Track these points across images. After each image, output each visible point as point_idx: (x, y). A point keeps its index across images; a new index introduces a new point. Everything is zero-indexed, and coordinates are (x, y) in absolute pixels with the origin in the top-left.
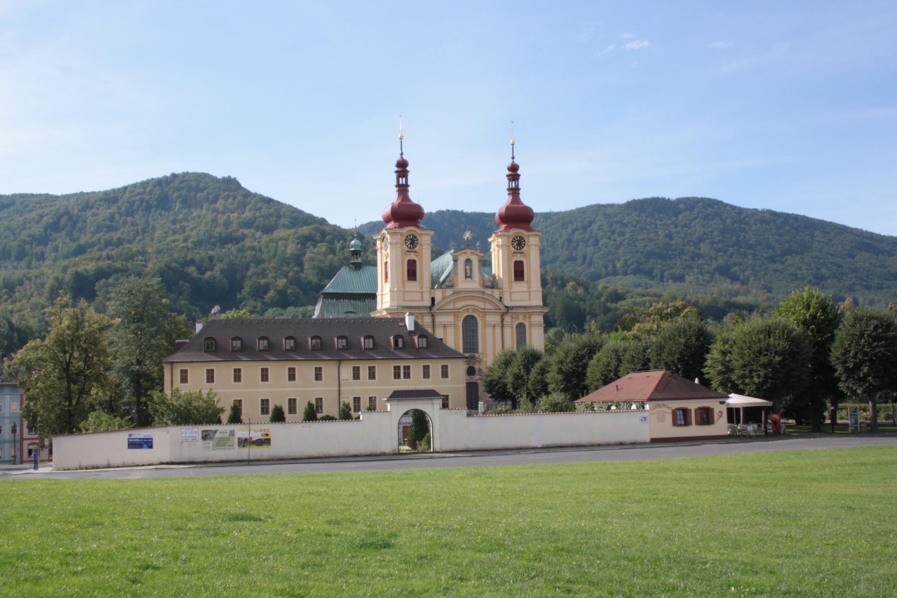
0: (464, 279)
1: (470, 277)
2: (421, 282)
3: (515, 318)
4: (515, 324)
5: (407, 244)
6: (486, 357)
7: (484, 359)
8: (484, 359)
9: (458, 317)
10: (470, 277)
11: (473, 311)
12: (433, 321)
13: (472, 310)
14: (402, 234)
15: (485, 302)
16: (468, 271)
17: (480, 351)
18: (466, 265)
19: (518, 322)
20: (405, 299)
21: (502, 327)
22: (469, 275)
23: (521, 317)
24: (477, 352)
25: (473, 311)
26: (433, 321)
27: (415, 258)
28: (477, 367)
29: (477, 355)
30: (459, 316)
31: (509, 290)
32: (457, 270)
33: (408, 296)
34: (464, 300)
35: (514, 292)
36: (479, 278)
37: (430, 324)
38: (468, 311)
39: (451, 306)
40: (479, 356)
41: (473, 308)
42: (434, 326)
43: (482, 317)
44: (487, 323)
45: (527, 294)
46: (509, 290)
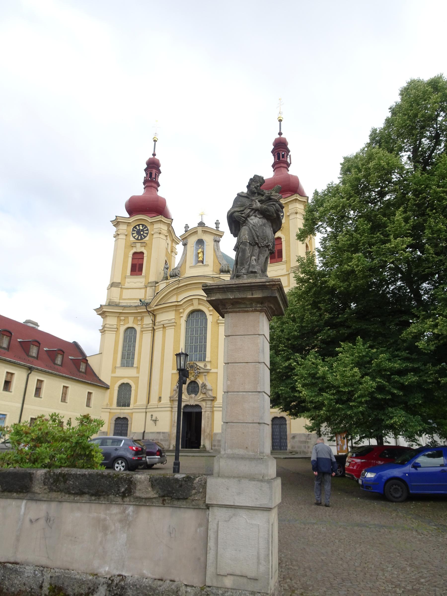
0: (193, 264)
1: (202, 262)
5: (134, 235)
6: (217, 368)
7: (213, 370)
8: (213, 370)
11: (199, 304)
13: (197, 300)
18: (197, 249)
22: (201, 259)
25: (199, 304)
28: (200, 381)
29: (201, 365)
30: (181, 311)
32: (186, 255)
33: (127, 294)
34: (190, 289)
37: (151, 325)
38: (192, 304)
39: (174, 299)
40: (205, 366)
41: (199, 299)
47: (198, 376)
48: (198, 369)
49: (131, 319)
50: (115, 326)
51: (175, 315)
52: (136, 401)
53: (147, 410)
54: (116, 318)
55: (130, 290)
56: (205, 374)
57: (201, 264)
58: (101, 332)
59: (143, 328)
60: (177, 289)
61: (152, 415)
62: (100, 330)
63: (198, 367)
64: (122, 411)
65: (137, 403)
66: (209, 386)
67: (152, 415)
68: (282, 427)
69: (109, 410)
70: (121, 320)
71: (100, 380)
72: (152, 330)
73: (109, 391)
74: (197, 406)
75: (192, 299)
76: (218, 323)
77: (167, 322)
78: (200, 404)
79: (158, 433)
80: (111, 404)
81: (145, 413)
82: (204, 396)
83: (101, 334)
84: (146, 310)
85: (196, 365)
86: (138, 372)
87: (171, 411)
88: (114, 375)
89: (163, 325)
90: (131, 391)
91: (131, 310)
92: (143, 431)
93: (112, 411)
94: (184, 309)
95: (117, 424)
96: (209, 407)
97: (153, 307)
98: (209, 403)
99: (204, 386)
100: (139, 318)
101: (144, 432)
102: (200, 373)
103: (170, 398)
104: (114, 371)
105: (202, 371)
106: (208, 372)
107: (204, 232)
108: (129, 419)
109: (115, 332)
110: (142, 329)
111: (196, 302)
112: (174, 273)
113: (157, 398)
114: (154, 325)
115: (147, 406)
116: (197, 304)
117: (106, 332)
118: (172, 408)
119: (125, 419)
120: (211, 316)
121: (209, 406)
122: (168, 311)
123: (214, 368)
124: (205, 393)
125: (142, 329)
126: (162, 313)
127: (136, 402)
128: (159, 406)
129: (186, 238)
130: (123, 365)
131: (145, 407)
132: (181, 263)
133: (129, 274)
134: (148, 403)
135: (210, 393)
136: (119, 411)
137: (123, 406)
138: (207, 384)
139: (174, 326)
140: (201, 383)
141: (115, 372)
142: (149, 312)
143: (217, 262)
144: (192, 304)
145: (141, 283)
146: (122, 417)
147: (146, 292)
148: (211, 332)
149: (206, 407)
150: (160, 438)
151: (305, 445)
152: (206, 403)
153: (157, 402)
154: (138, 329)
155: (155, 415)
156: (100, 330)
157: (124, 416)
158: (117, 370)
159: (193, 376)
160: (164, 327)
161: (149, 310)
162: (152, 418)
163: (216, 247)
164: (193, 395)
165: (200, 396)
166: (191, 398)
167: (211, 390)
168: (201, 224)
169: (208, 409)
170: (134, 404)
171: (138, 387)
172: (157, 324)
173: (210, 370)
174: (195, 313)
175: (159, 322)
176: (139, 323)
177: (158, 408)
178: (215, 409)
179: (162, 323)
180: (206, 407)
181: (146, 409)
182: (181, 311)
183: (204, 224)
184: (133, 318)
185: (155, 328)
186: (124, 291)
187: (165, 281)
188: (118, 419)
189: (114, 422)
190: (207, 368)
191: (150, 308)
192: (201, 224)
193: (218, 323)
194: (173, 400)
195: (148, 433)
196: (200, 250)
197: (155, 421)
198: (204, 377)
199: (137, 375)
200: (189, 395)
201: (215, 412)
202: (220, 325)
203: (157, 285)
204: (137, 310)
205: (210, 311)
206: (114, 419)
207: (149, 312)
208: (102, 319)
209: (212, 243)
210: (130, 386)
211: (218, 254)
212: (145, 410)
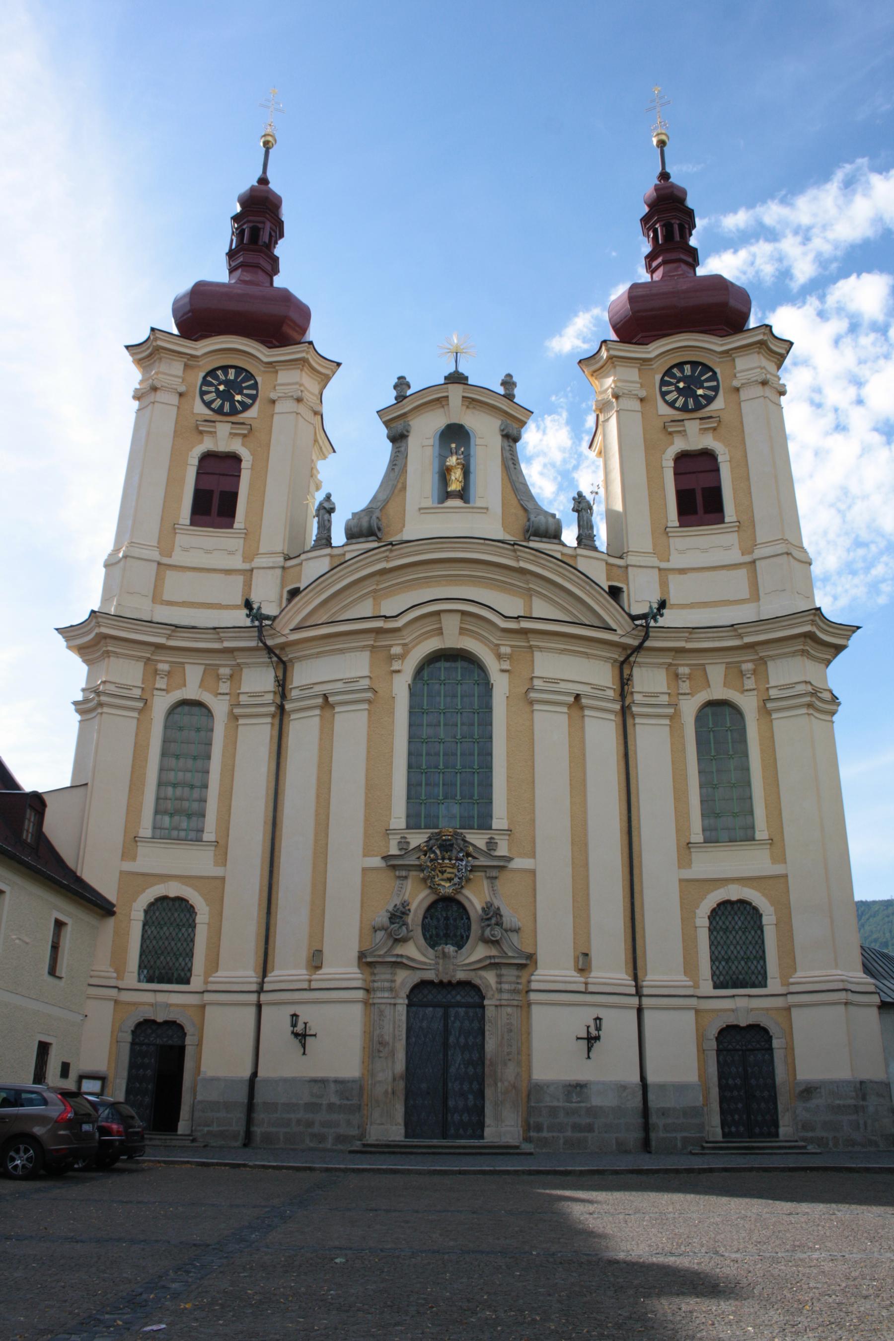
2: (251, 536)
3: (690, 677)
4: (689, 708)
6: (533, 856)
8: (519, 863)
9: (392, 658)
10: (463, 495)
11: (463, 631)
12: (282, 685)
14: (190, 361)
15: (529, 594)
16: (457, 475)
17: (500, 820)
19: (703, 697)
20: (166, 597)
21: (625, 713)
23: (716, 672)
24: (485, 823)
25: (463, 631)
26: (282, 685)
27: (236, 446)
29: (478, 839)
30: (396, 650)
31: (655, 561)
32: (404, 470)
34: (427, 581)
35: (682, 571)
36: (504, 504)
37: (269, 698)
38: (440, 632)
40: (492, 844)
41: (463, 613)
42: (281, 708)
43: (510, 657)
44: (537, 683)
45: (743, 573)
46: (655, 561)
47: (468, 880)
48: (468, 855)
49: (194, 673)
50: (137, 693)
51: (372, 665)
52: (213, 964)
53: (264, 997)
54: (140, 665)
55: (190, 574)
56: (494, 873)
57: (457, 503)
58: (80, 711)
59: (238, 705)
60: (377, 578)
61: (295, 1016)
62: (75, 703)
63: (471, 849)
64: (161, 998)
65: (219, 974)
66: (510, 917)
67: (295, 1016)
68: (752, 1058)
69: (114, 992)
70: (156, 672)
71: (79, 880)
72: (273, 716)
73: (111, 921)
74: (467, 985)
75: (438, 613)
76: (531, 703)
77: (339, 686)
78: (477, 981)
79: (315, 1081)
80: (120, 972)
81: (253, 1010)
82: (494, 952)
83: (78, 717)
84: (253, 644)
85: (464, 841)
86: (222, 857)
87: (366, 1003)
88: (128, 866)
89: (325, 697)
90: (193, 926)
91: (196, 640)
92: (247, 1073)
93: (126, 997)
94: (404, 645)
95: (141, 1044)
96: (509, 991)
97: (284, 633)
98: (510, 974)
99: (492, 915)
100: (225, 671)
101: (255, 1074)
102: (474, 869)
103: (362, 955)
104: (129, 854)
105: (483, 861)
106: (502, 868)
107: (471, 402)
108: (189, 1029)
109: (136, 715)
110: (237, 711)
111: (451, 624)
112: (365, 523)
113: (303, 955)
114: (283, 696)
115: (262, 984)
116: (457, 631)
117: (105, 710)
118: (367, 991)
119: (175, 1027)
120: (506, 675)
121: (513, 987)
122: (341, 651)
123: (523, 855)
124: (496, 943)
125: (237, 711)
126: (318, 655)
127: (216, 968)
128: (314, 985)
129: (404, 415)
130: (161, 834)
131: (254, 987)
132: (382, 497)
133: (188, 522)
134: (264, 975)
135: (514, 938)
136: (149, 998)
137: (161, 981)
138: (503, 911)
139: (369, 702)
140: (479, 907)
141: (134, 858)
142: (270, 650)
143: (515, 502)
144: (440, 632)
145: (231, 553)
146: (160, 1019)
147: (248, 585)
148: (508, 730)
149: (500, 991)
150: (325, 1102)
151: (854, 1117)
152: (499, 976)
153: (302, 972)
154: (220, 708)
155: (306, 1014)
156: (75, 703)
157: (171, 1017)
158: (142, 850)
159: (450, 880)
160: (326, 703)
161: (270, 643)
162: (294, 1025)
163: (508, 455)
164: (450, 949)
165: (479, 952)
166: (445, 955)
167: (517, 931)
168: (457, 378)
169: (505, 996)
170: (207, 974)
171: (221, 914)
172: (294, 694)
173: (509, 859)
174: (443, 665)
175: (302, 688)
176: (224, 687)
177: (311, 990)
178: (533, 996)
179: (318, 689)
180: (500, 991)
181: (260, 991)
182: (396, 650)
183: (466, 378)
184: (202, 668)
185: (288, 706)
186: (169, 574)
187: (328, 551)
188: (145, 1026)
189: (129, 1038)
190: (497, 853)
191: (272, 636)
192: (457, 378)
193: (531, 703)
194: (370, 964)
195: (267, 1081)
196: (452, 461)
197: (302, 1037)
198: (486, 882)
199: (218, 872)
200: (432, 946)
201: (535, 1009)
202: (536, 707)
203: (290, 563)
204: (221, 640)
205: (499, 657)
206: (131, 1024)
207: (270, 650)
208: (84, 668)
209: (497, 441)
210: (190, 910)
211: (514, 478)
212: (253, 998)
